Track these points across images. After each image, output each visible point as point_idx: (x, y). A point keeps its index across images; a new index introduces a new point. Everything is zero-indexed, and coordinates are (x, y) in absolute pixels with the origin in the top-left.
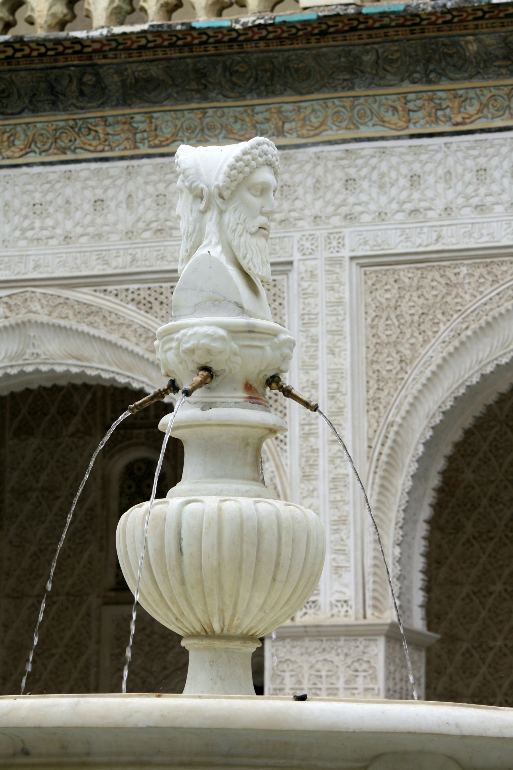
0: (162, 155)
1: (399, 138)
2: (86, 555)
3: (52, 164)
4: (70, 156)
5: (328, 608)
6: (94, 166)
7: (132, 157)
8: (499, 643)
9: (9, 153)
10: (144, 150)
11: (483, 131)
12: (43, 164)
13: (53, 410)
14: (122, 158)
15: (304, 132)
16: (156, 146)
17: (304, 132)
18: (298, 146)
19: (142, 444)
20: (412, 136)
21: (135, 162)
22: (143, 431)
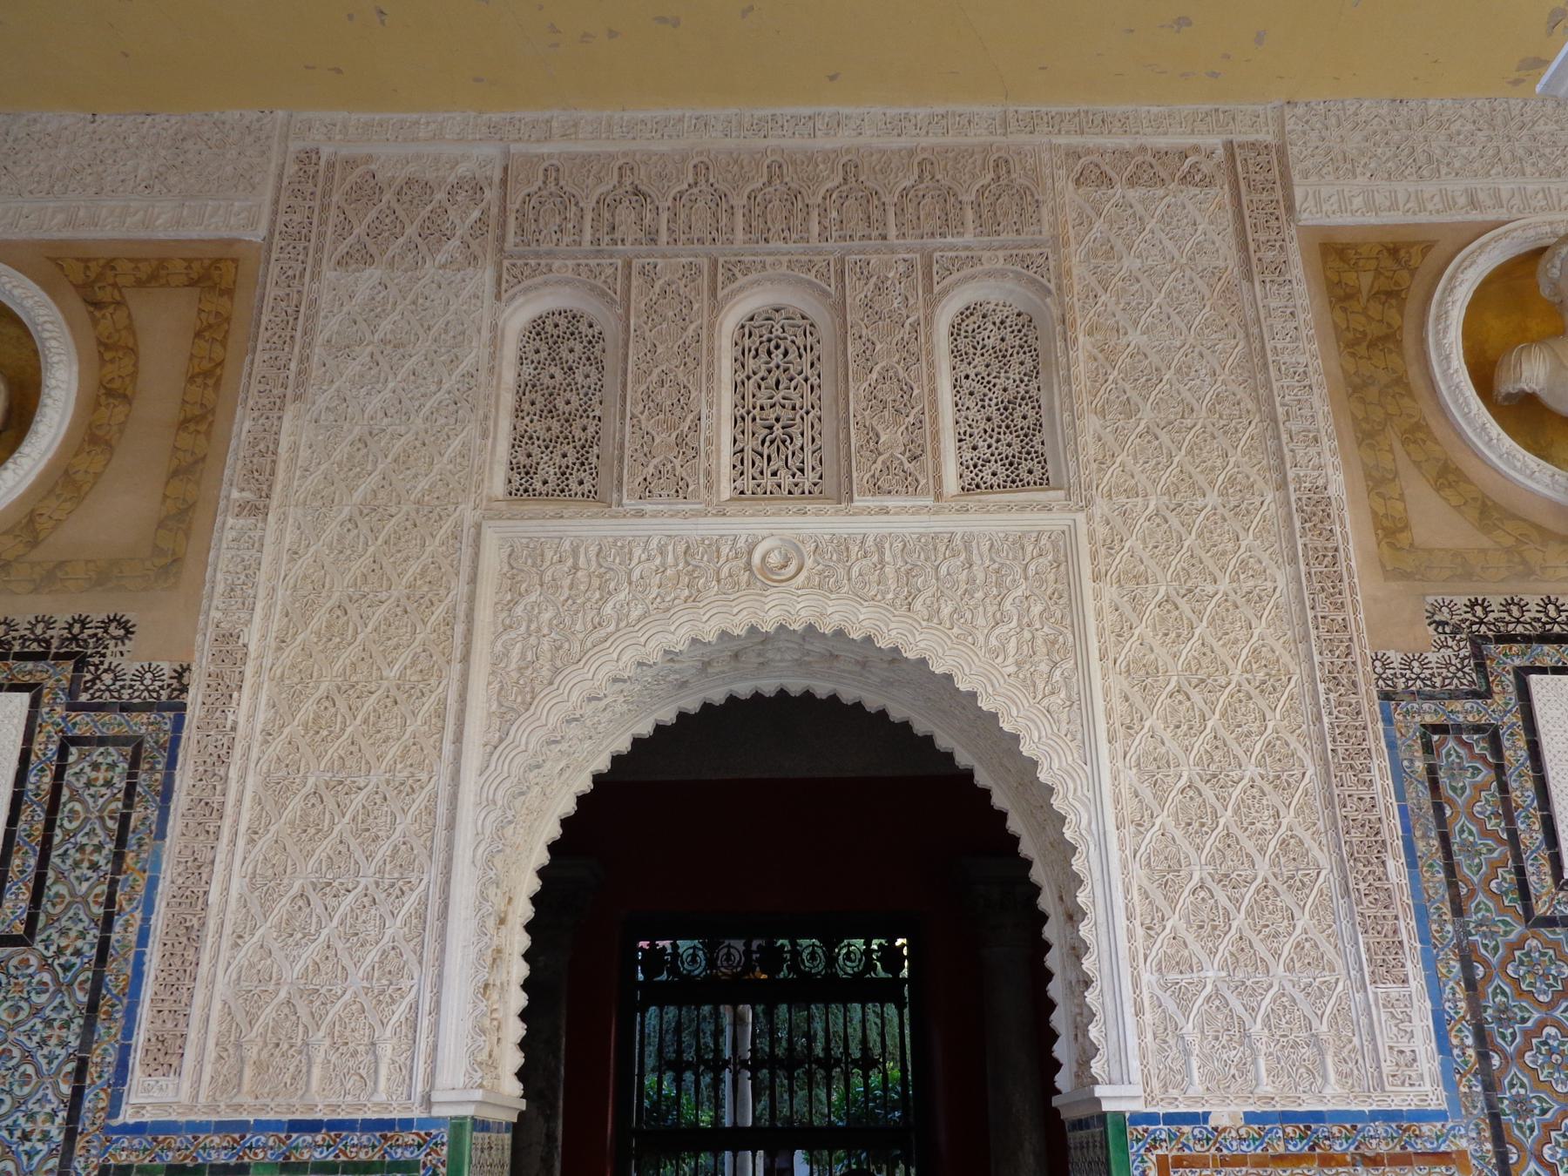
2: (456, 444)
8: (1224, 585)
13: (411, 230)
19: (568, 282)
22: (570, 263)
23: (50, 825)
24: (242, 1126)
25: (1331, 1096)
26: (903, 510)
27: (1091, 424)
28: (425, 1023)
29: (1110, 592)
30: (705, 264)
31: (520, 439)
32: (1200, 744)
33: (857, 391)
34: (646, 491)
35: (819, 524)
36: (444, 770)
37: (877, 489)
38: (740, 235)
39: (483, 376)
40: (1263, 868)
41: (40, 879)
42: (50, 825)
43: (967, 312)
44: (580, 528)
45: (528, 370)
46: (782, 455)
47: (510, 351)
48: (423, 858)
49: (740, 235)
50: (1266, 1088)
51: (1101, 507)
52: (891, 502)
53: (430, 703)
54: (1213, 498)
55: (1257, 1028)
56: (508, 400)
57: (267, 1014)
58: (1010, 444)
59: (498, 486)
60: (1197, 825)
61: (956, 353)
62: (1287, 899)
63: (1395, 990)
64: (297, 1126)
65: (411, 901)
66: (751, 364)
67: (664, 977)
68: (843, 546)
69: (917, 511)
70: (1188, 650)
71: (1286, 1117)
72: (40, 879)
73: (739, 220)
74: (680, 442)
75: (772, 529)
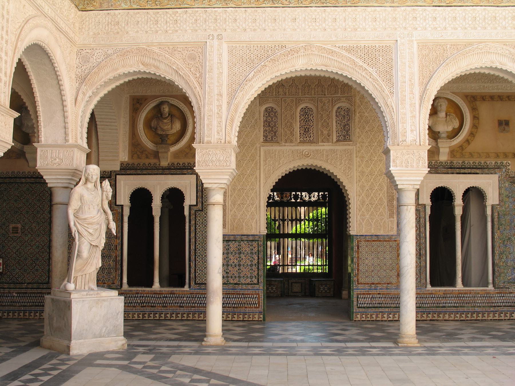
0: (355, 6)
1: (429, 6)
3: (319, 7)
4: (325, 5)
5: (410, 142)
6: (332, 8)
7: (345, 7)
8: (376, 158)
9: (305, 3)
10: (349, 4)
11: (455, 6)
12: (316, 7)
14: (342, 7)
15: (400, 2)
16: (353, 4)
17: (400, 2)
18: (398, 7)
20: (433, 6)
21: (346, 8)
23: (202, 194)
24: (235, 235)
25: (381, 233)
26: (327, 145)
27: (358, 130)
28: (258, 222)
29: (358, 159)
30: (294, 99)
31: (265, 131)
32: (370, 184)
33: (320, 124)
34: (286, 142)
35: (313, 147)
36: (258, 186)
37: (323, 142)
38: (300, 94)
39: (258, 120)
40: (376, 202)
41: (202, 202)
42: (202, 194)
43: (338, 108)
44: (276, 148)
45: (265, 118)
46: (307, 135)
47: (262, 115)
48: (256, 199)
49: (300, 94)
50: (373, 232)
51: (358, 145)
52: (325, 144)
53: (255, 176)
54: (376, 144)
55: (373, 224)
56: (262, 124)
57: (236, 221)
58: (344, 133)
59: (262, 140)
60: (367, 196)
61: (336, 116)
62: (379, 206)
63: (392, 219)
64: (242, 235)
65: (255, 205)
66: (302, 117)
67: (271, 201)
68: (317, 151)
69: (329, 145)
70: (369, 169)
71: (375, 235)
72: (202, 202)
73: (300, 91)
74: (291, 133)
75: (306, 148)
